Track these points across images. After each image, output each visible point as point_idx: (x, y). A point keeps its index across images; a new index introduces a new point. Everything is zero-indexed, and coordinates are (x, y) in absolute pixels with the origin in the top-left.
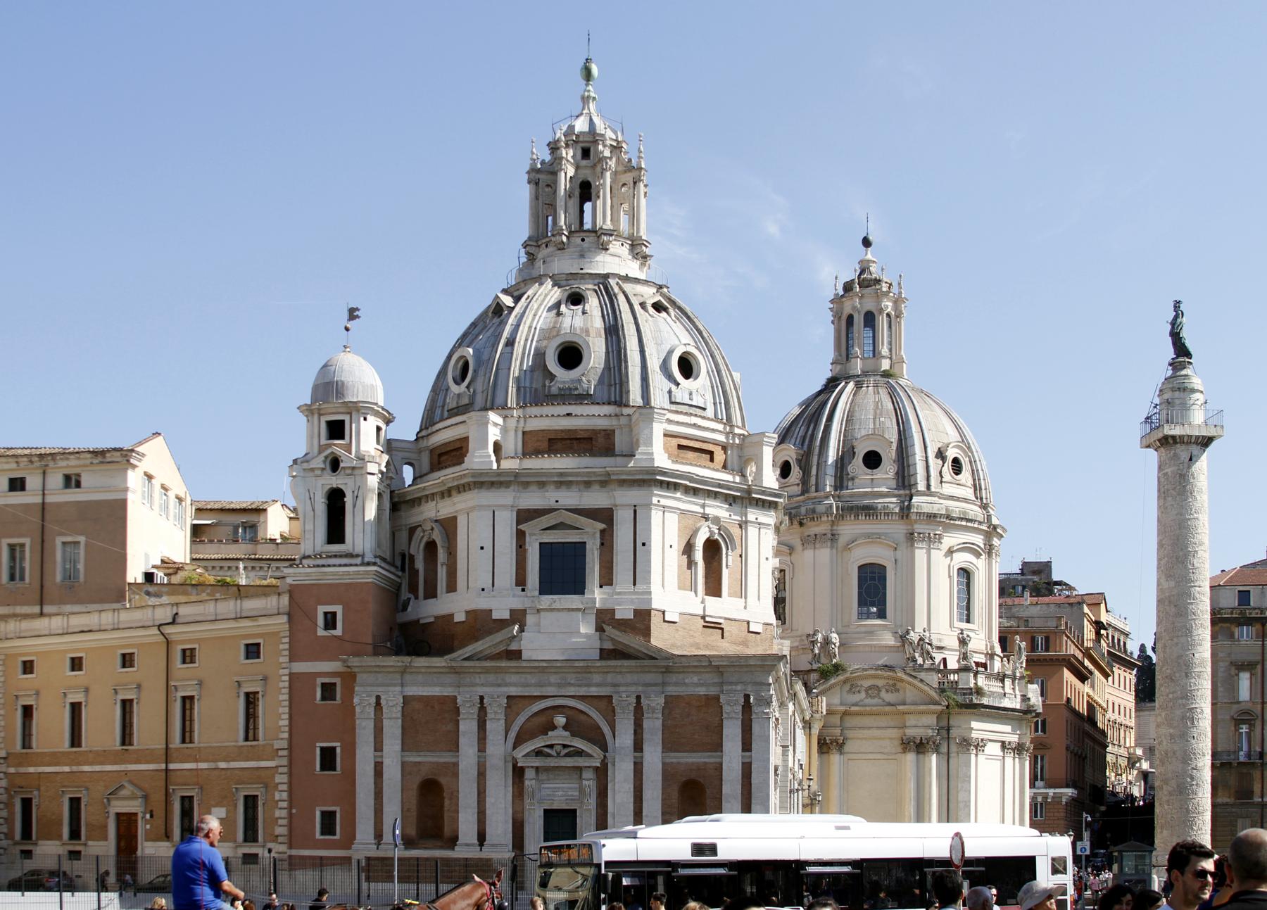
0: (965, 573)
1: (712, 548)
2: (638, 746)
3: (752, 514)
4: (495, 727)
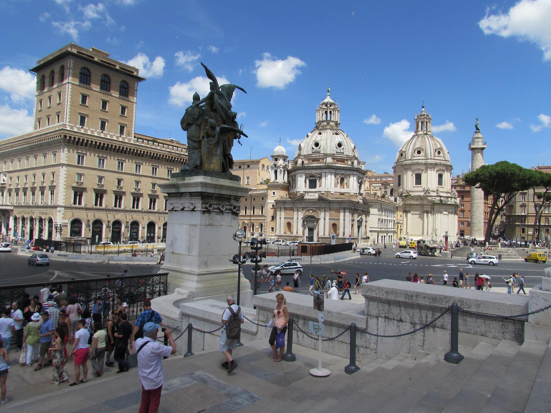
2: (325, 217)
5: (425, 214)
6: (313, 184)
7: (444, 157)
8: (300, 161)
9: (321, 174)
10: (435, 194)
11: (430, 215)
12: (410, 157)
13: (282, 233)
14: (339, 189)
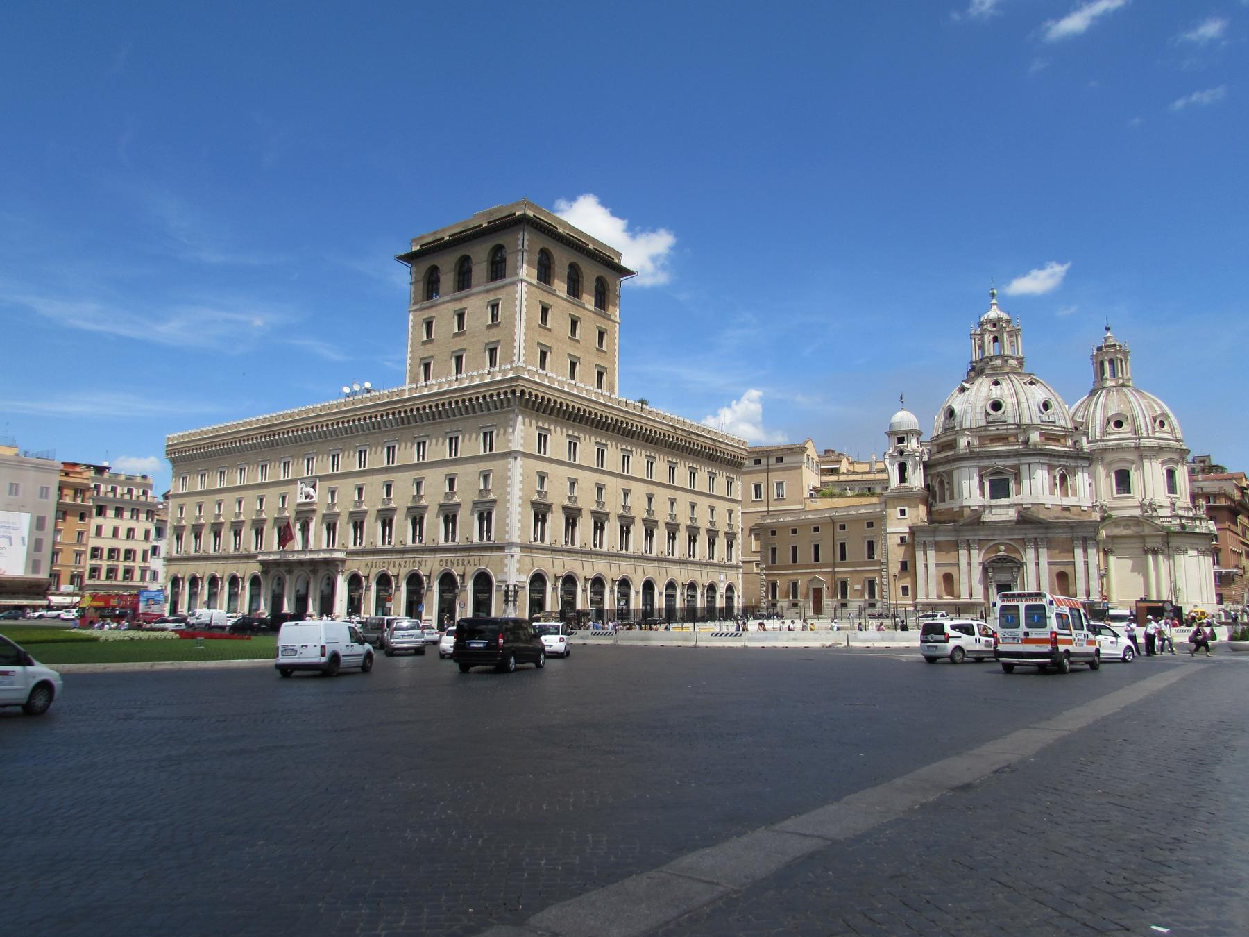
3: (1080, 463)
4: (974, 553)
5: (1150, 557)
6: (1000, 489)
7: (1172, 432)
8: (963, 442)
9: (1018, 468)
10: (1167, 512)
11: (1161, 558)
12: (1098, 434)
13: (933, 598)
14: (1058, 499)
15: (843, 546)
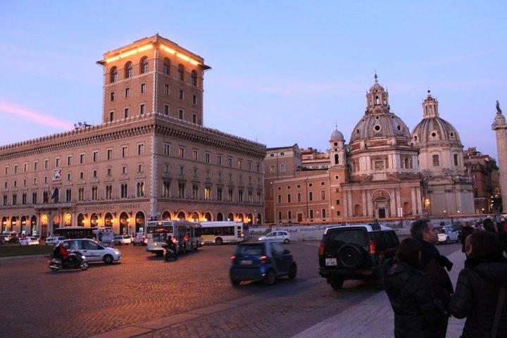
0: (455, 156)
1: (406, 160)
2: (395, 197)
4: (369, 195)
15: (311, 193)
